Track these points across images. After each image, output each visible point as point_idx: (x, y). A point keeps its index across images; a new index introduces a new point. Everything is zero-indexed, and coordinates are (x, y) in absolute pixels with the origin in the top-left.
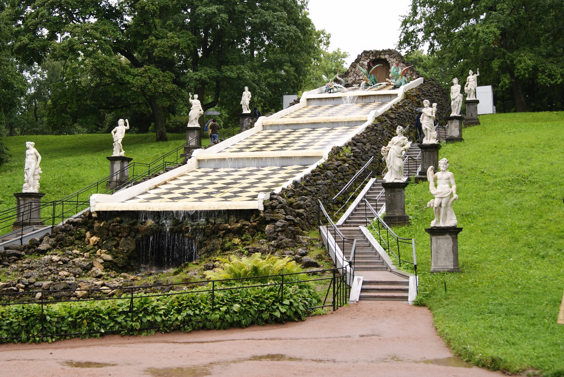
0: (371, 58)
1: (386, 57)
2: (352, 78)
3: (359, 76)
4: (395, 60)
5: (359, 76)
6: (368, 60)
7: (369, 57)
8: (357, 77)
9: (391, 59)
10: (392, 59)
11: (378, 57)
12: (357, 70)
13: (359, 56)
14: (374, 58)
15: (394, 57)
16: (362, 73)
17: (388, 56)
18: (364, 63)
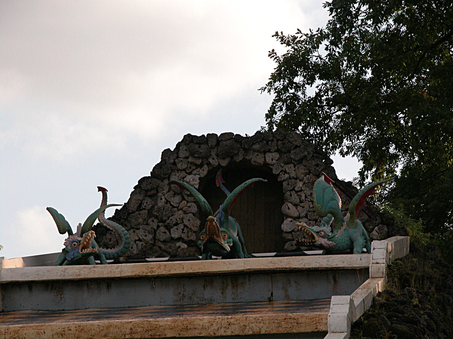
0: (214, 162)
1: (269, 160)
2: (141, 233)
3: (168, 228)
4: (301, 170)
5: (168, 228)
6: (204, 171)
7: (207, 157)
8: (162, 229)
9: (287, 168)
10: (290, 168)
11: (239, 158)
12: (161, 203)
13: (166, 153)
14: (224, 163)
15: (300, 162)
16: (179, 214)
17: (277, 155)
18: (189, 178)
